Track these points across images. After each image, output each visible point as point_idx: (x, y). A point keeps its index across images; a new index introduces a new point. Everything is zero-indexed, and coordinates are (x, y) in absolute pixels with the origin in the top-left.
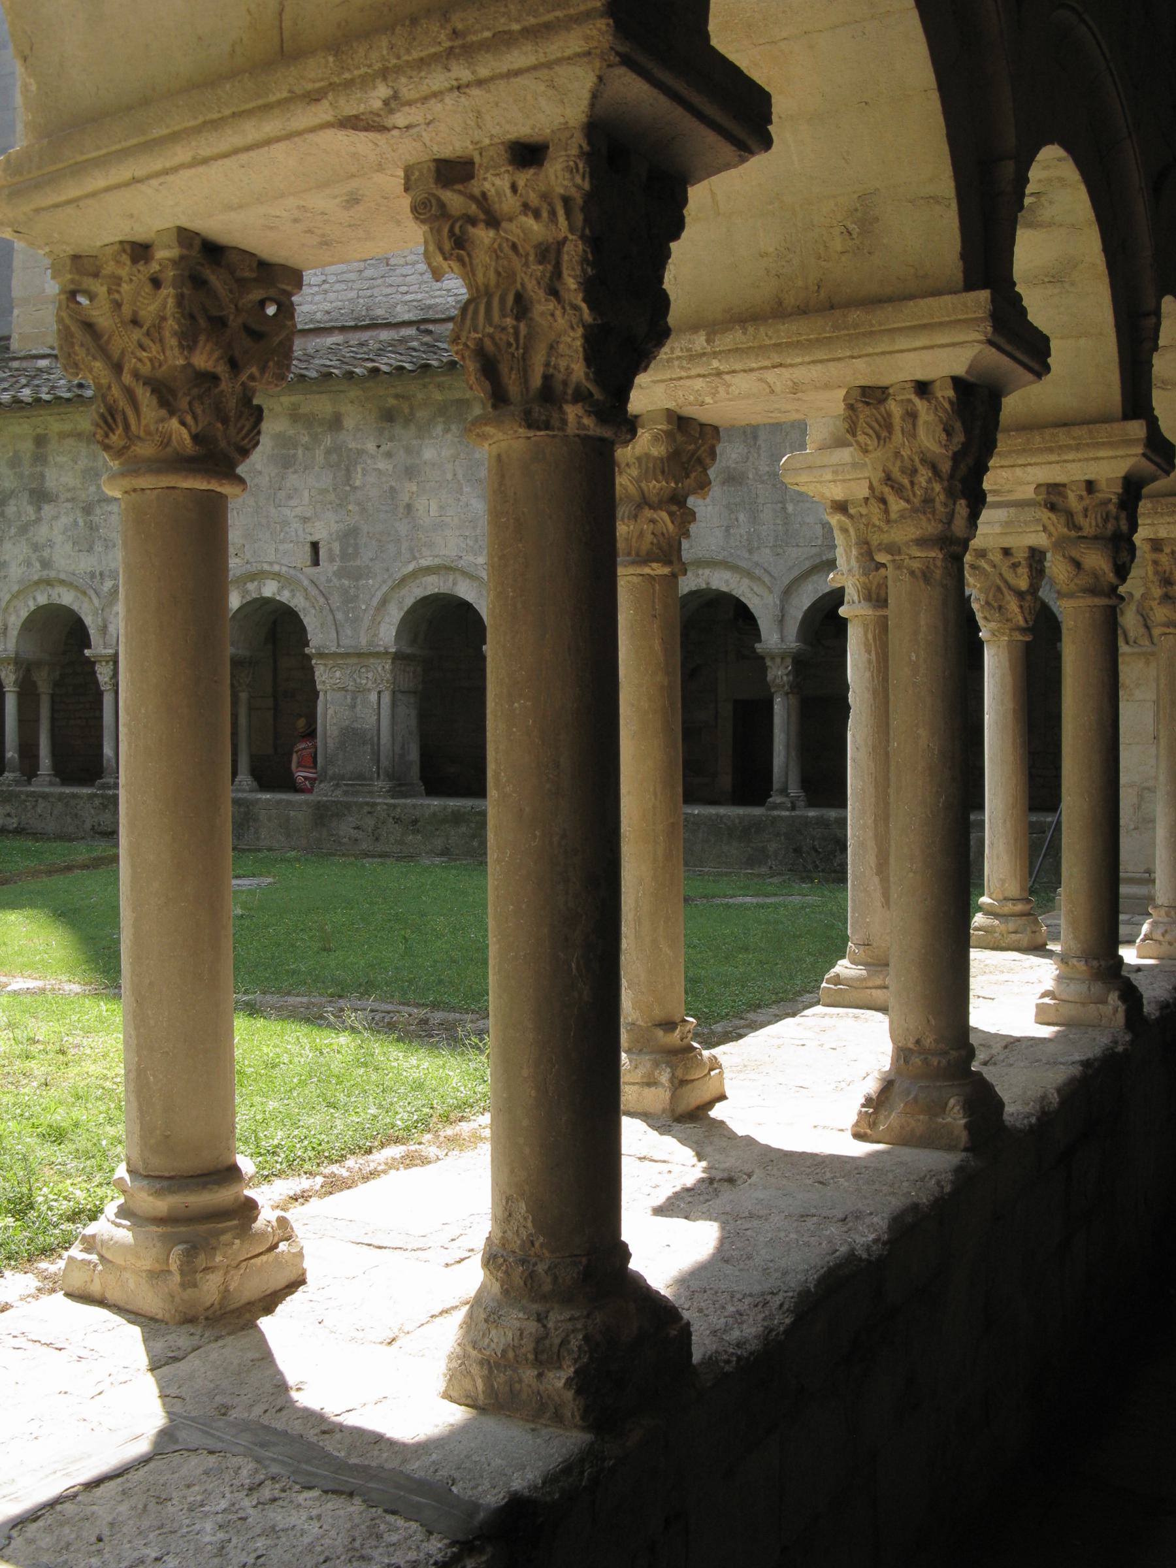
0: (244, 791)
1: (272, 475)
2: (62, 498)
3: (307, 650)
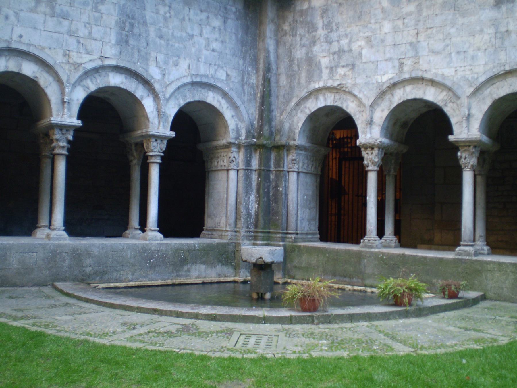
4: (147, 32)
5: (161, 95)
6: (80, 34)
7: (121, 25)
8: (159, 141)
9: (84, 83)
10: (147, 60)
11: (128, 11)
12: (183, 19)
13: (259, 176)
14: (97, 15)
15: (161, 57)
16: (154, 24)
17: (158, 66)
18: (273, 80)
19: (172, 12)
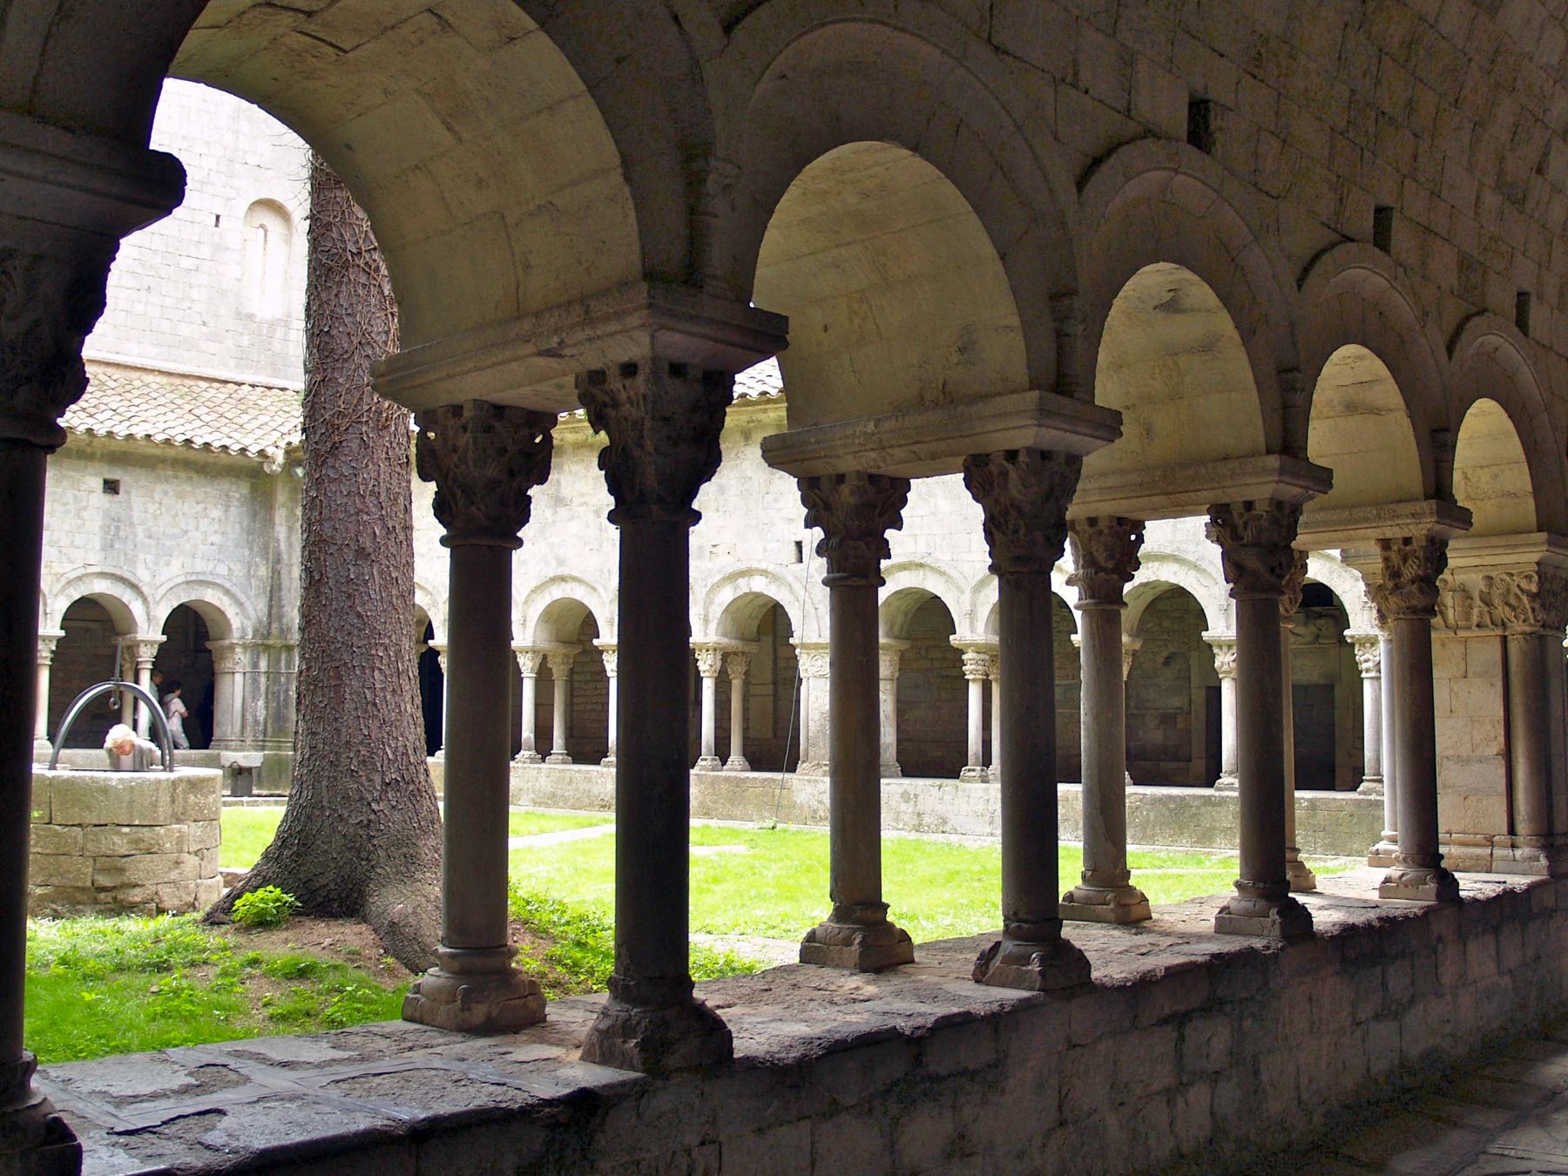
0: (736, 770)
1: (761, 481)
2: (576, 502)
3: (791, 641)
4: (134, 533)
5: (149, 599)
6: (62, 544)
7: (105, 529)
8: (149, 646)
9: (67, 592)
10: (135, 562)
11: (113, 514)
12: (176, 515)
13: (268, 678)
14: (79, 522)
15: (150, 558)
16: (142, 524)
17: (147, 568)
18: (284, 572)
19: (163, 509)
